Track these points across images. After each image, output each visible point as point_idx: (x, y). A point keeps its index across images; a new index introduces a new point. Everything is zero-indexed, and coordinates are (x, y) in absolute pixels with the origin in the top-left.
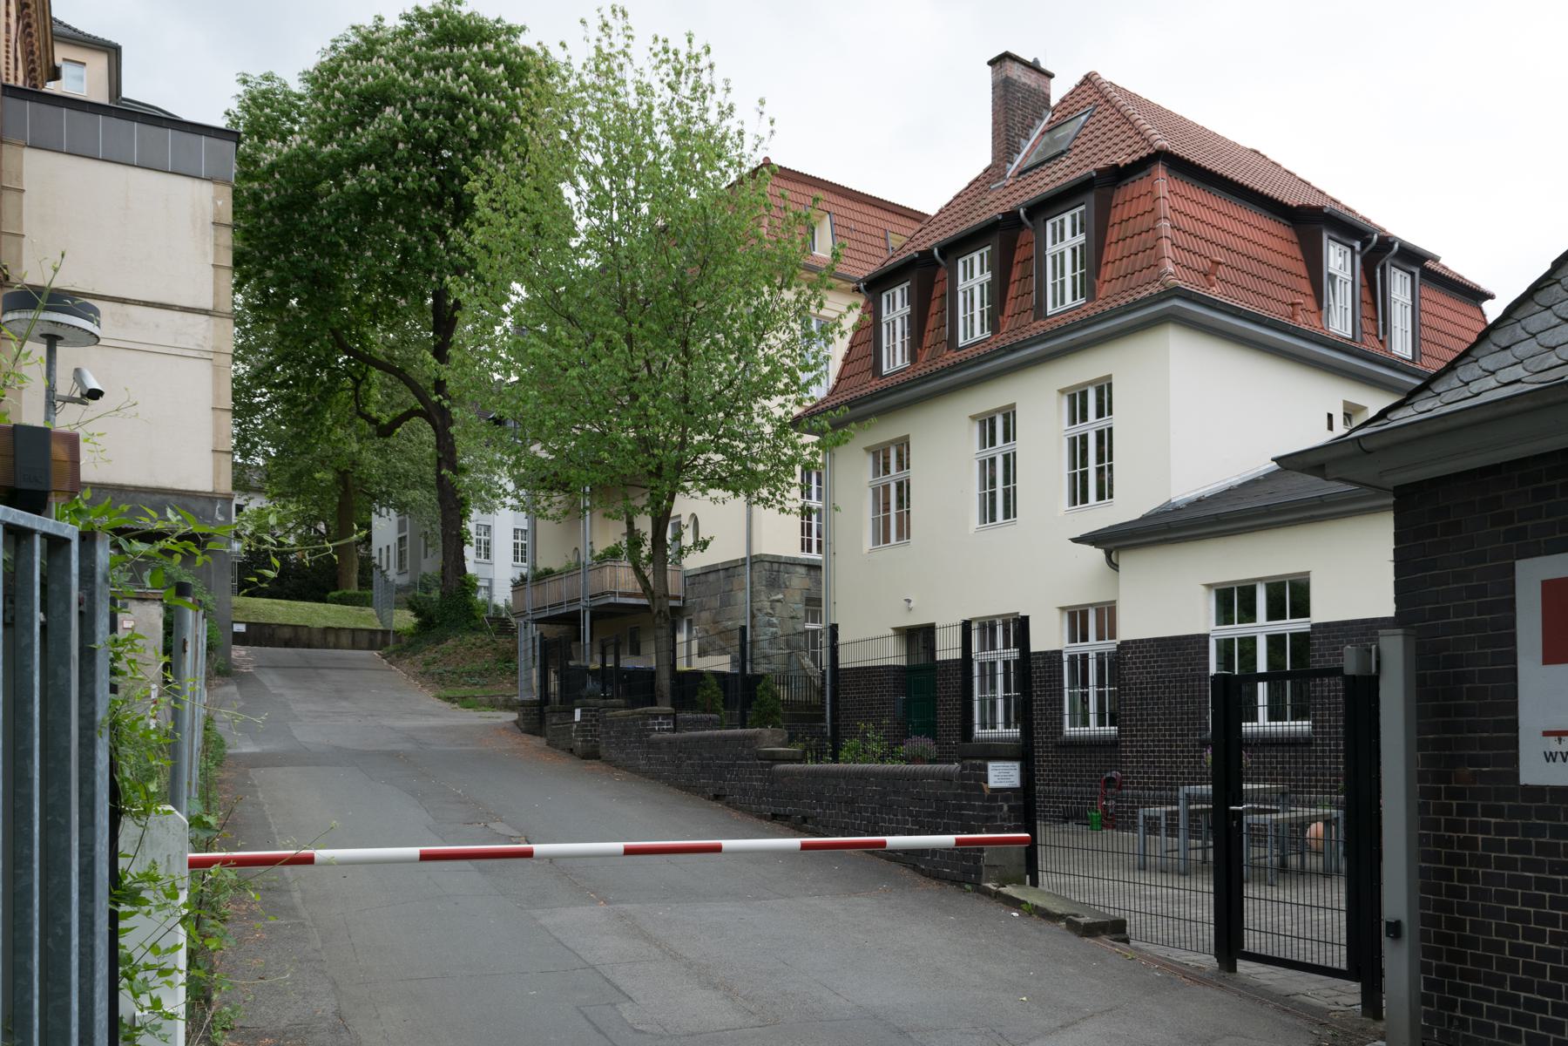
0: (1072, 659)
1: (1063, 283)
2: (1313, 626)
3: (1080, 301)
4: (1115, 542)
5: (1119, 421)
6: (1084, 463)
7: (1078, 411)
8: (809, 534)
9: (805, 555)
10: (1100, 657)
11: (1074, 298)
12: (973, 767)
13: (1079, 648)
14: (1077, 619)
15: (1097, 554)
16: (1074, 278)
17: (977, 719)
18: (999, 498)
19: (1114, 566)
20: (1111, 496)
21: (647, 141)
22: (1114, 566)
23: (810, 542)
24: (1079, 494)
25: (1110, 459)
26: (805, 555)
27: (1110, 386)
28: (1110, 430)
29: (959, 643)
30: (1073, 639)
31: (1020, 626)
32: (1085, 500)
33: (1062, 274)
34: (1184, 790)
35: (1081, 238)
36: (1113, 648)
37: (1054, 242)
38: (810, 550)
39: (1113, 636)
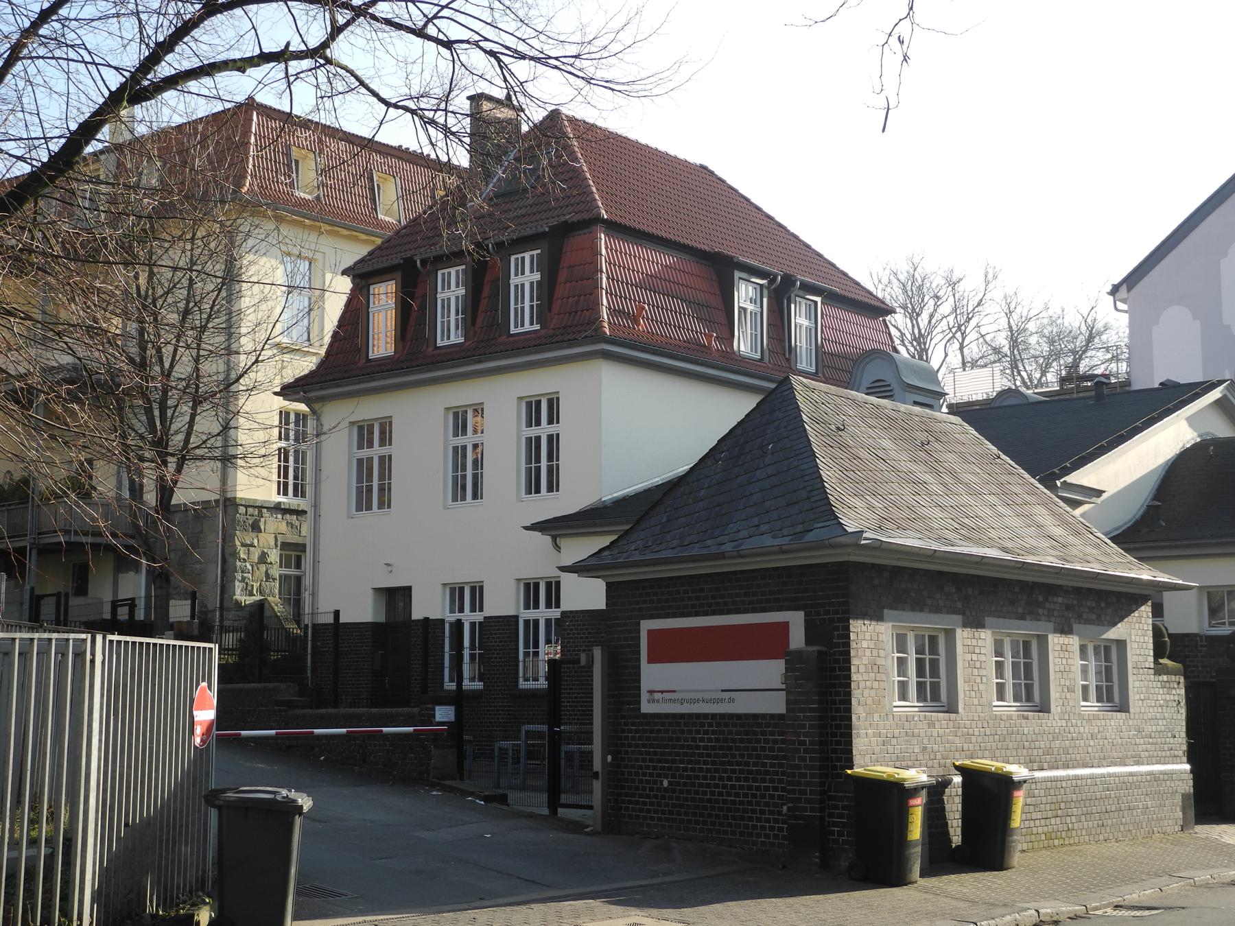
0: (527, 622)
1: (523, 309)
2: (563, 613)
3: (537, 327)
4: (557, 528)
5: (396, 450)
6: (538, 460)
7: (533, 416)
8: (286, 476)
9: (281, 499)
10: (548, 621)
11: (532, 323)
12: (428, 709)
13: (531, 614)
14: (530, 592)
15: (544, 540)
16: (532, 307)
17: (521, 674)
18: (466, 481)
19: (557, 548)
20: (389, 506)
21: (123, 11)
22: (557, 548)
23: (286, 485)
24: (533, 486)
25: (390, 478)
26: (281, 499)
27: (391, 423)
28: (390, 457)
29: (54, 611)
30: (527, 607)
31: (477, 591)
32: (538, 491)
33: (523, 303)
34: (525, 728)
35: (537, 276)
36: (558, 615)
37: (516, 275)
38: (285, 494)
39: (558, 606)
